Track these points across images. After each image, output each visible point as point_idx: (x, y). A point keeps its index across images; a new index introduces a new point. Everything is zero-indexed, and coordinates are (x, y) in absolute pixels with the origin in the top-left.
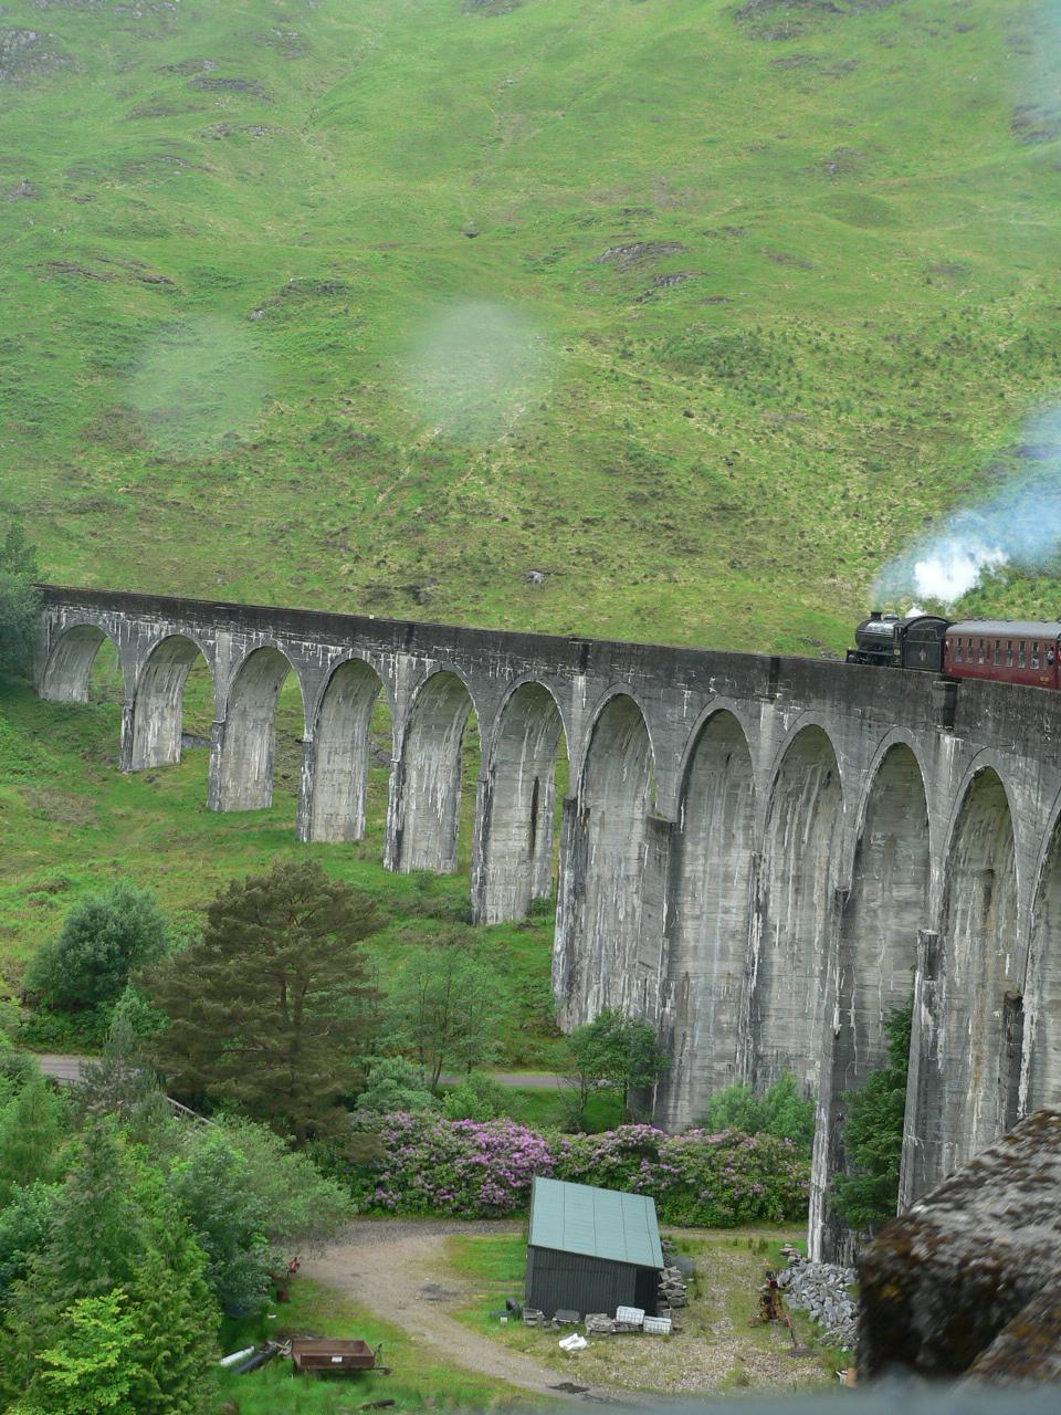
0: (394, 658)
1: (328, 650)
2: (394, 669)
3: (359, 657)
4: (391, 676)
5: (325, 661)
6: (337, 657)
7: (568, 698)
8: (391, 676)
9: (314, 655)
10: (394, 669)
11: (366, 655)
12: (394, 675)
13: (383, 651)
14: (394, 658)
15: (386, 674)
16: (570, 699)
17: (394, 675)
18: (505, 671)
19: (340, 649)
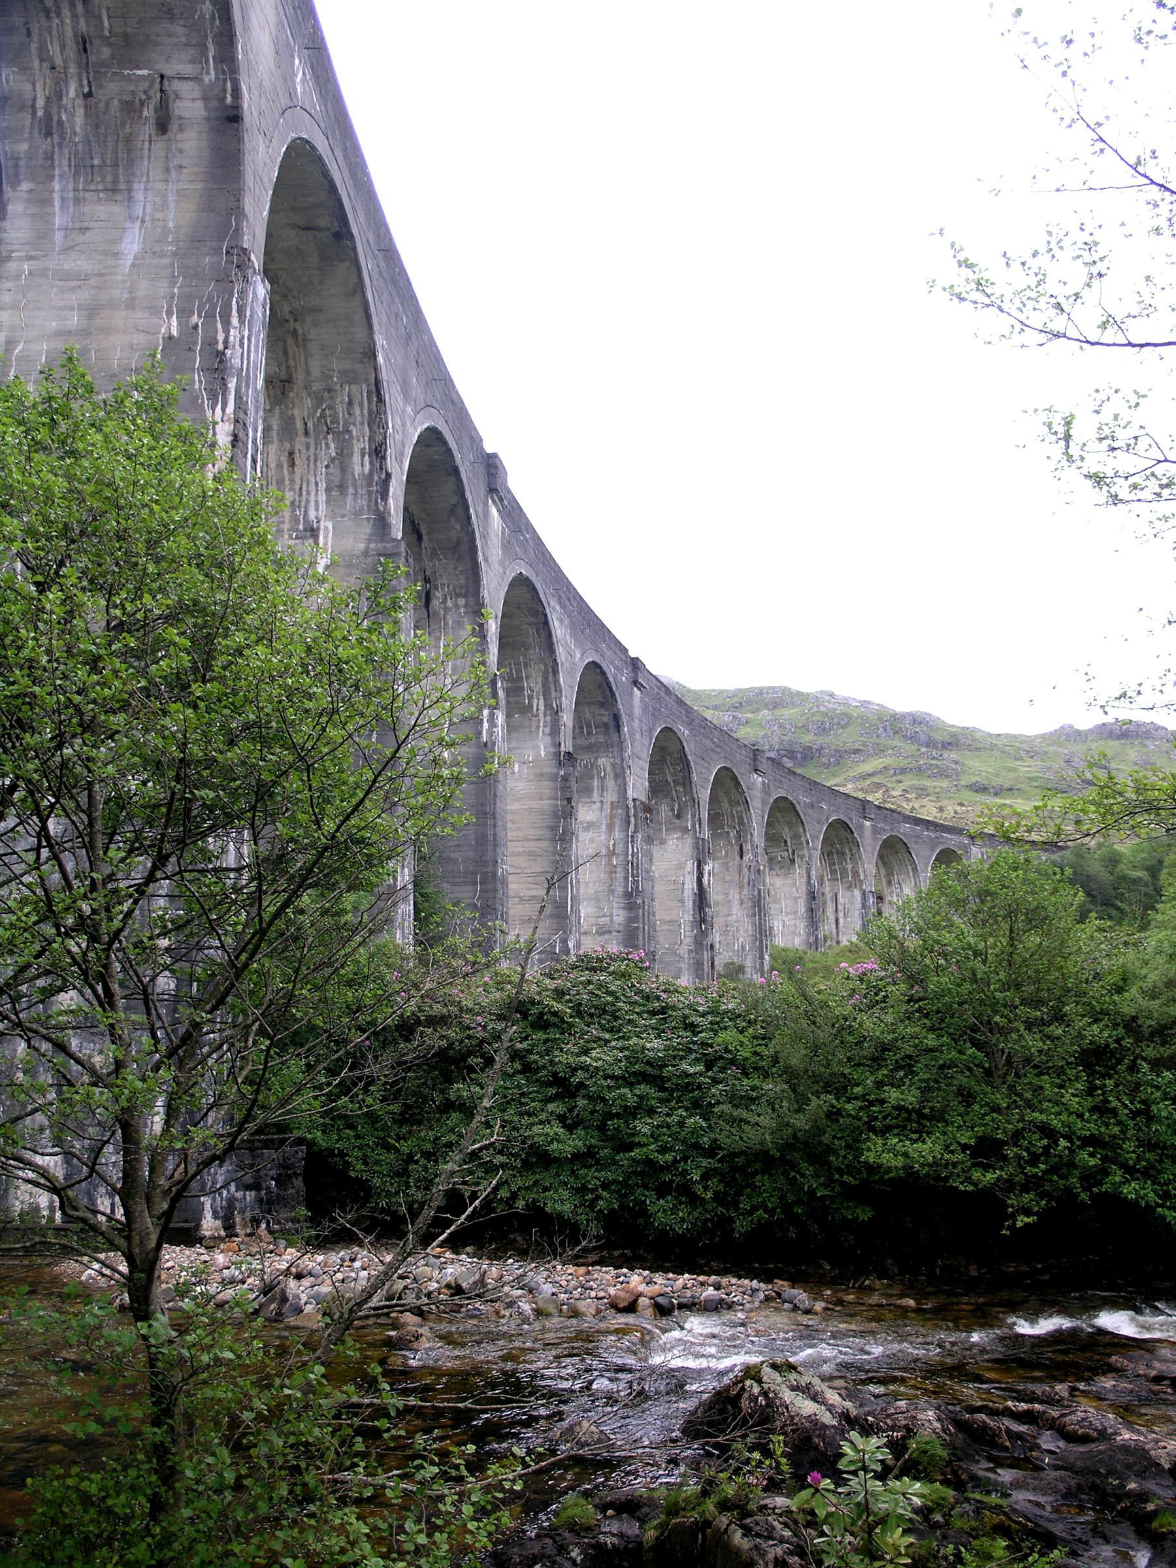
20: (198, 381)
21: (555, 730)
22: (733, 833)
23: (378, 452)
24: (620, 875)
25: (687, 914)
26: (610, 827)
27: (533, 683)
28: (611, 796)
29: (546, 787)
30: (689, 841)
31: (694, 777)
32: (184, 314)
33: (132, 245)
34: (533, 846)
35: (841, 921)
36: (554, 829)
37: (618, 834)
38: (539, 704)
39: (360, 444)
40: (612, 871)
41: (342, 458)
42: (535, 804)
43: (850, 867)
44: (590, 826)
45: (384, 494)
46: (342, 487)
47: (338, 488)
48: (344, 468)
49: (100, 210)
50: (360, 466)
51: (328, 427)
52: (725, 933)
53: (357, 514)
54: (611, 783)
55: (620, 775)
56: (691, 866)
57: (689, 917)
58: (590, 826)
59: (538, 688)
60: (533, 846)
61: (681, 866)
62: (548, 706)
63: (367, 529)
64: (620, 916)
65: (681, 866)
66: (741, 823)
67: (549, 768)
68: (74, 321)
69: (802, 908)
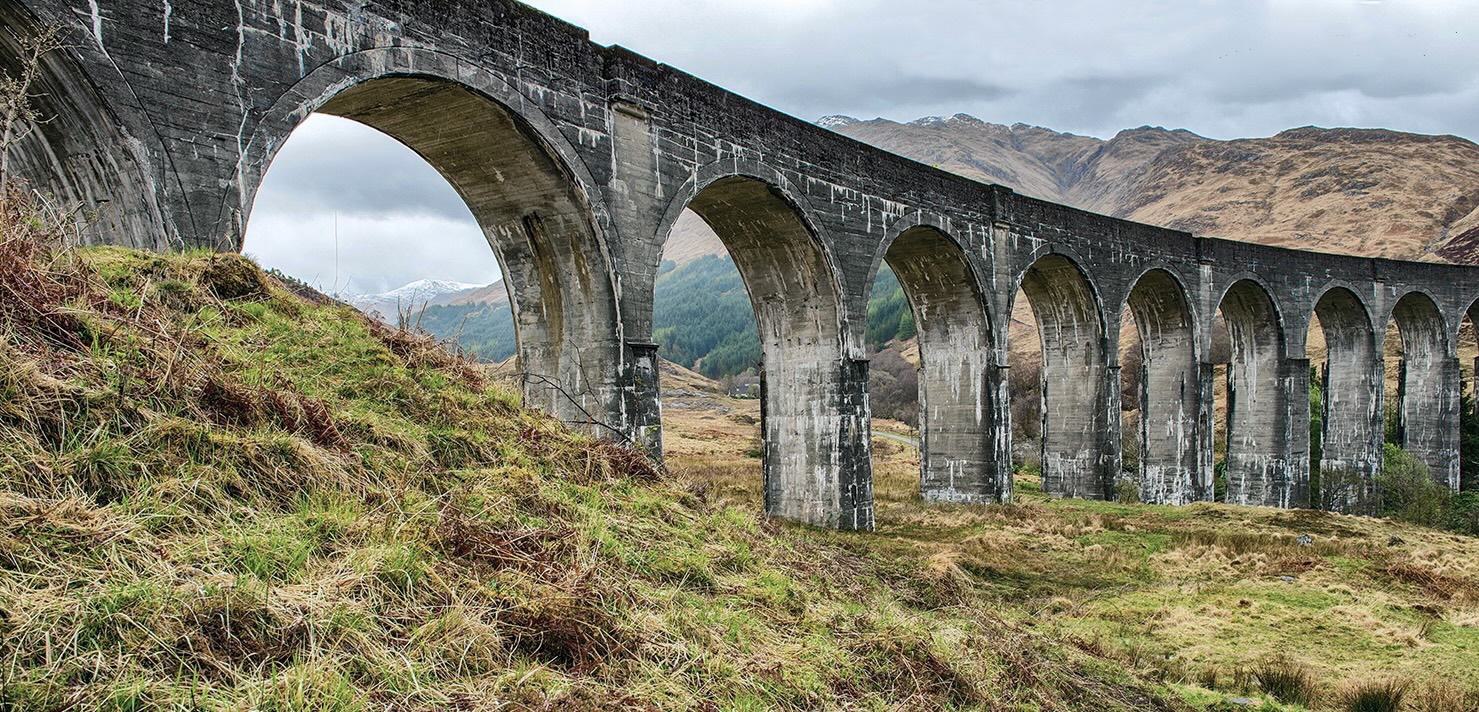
0: (987, 231)
1: (881, 207)
2: (988, 246)
3: (933, 224)
4: (985, 256)
5: (877, 223)
6: (896, 219)
7: (1197, 280)
8: (985, 256)
9: (856, 210)
10: (988, 246)
11: (944, 223)
12: (989, 256)
13: (970, 220)
14: (987, 231)
15: (977, 252)
16: (1198, 284)
17: (989, 256)
18: (1129, 257)
19: (901, 207)
20: (1368, 388)
23: (1443, 334)
32: (1365, 374)
33: (1354, 359)
41: (1433, 336)
45: (1447, 345)
46: (1434, 343)
47: (1433, 343)
49: (1347, 352)
50: (1439, 338)
51: (1426, 329)
53: (1439, 351)
63: (1442, 355)
68: (1344, 376)
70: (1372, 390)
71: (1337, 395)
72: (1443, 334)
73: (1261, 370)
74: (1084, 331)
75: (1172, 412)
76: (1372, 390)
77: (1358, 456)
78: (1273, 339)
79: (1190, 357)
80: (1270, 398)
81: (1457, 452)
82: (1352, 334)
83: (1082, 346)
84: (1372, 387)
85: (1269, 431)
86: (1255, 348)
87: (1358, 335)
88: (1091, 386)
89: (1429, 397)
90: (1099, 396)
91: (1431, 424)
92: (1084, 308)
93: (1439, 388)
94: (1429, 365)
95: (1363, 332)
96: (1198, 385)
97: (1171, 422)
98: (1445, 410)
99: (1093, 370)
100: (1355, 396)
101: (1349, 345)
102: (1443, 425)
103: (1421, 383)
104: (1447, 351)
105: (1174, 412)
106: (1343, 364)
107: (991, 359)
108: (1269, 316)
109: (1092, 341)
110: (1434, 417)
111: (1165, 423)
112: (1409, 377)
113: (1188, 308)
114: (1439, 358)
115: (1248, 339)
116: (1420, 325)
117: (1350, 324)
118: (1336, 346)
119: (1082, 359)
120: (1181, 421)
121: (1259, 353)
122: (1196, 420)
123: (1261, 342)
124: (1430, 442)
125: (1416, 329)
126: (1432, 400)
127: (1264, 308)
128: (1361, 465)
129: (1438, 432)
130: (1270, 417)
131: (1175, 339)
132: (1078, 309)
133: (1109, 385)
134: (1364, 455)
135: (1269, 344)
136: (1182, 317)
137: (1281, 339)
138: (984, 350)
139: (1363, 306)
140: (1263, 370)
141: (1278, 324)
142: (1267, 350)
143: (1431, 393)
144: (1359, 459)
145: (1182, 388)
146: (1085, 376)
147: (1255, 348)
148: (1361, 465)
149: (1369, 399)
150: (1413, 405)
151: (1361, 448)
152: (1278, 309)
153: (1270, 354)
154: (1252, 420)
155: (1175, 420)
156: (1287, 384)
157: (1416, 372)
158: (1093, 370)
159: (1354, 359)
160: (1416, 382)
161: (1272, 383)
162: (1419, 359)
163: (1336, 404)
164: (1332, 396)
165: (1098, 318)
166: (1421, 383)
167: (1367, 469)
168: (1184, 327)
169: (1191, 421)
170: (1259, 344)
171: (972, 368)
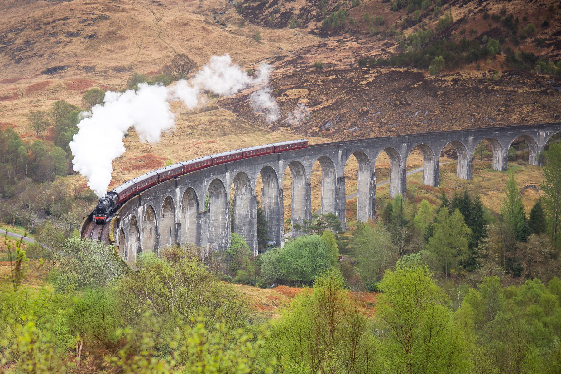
21: (306, 180)
22: (397, 160)
23: (250, 186)
24: (334, 194)
25: (367, 191)
26: (332, 184)
27: (301, 171)
28: (333, 177)
29: (304, 190)
30: (369, 173)
31: (369, 158)
33: (219, 203)
34: (302, 200)
35: (461, 169)
36: (305, 198)
37: (334, 185)
38: (302, 174)
39: (248, 185)
40: (333, 193)
42: (302, 193)
43: (464, 152)
44: (328, 183)
47: (247, 189)
48: (247, 187)
49: (217, 200)
50: (249, 187)
51: (244, 184)
52: (394, 187)
54: (332, 174)
55: (334, 172)
56: (369, 179)
57: (368, 192)
58: (328, 183)
59: (302, 172)
60: (302, 200)
61: (367, 179)
62: (304, 175)
63: (250, 195)
64: (334, 203)
65: (367, 179)
66: (398, 158)
67: (305, 186)
69: (432, 172)
70: (226, 216)
71: (213, 217)
72: (250, 186)
73: (191, 216)
74: (150, 223)
75: (167, 240)
76: (226, 216)
77: (222, 242)
78: (195, 205)
79: (173, 221)
80: (194, 227)
81: (256, 234)
82: (218, 193)
83: (149, 228)
84: (226, 214)
85: (194, 240)
86: (188, 208)
87: (221, 193)
88: (152, 241)
89: (245, 211)
90: (155, 245)
91: (246, 223)
92: (151, 217)
93: (249, 209)
94: (245, 198)
95: (223, 193)
96: (176, 231)
97: (167, 244)
98: (251, 218)
99: (153, 236)
100: (220, 217)
101: (217, 197)
102: (251, 223)
103: (242, 205)
104: (251, 193)
105: (168, 240)
106: (215, 204)
107: (139, 246)
108: (194, 197)
109: (153, 227)
110: (248, 220)
111: (165, 244)
112: (238, 202)
113: (173, 205)
114: (249, 196)
115: (186, 204)
116: (241, 182)
117: (218, 189)
118: (213, 197)
119: (149, 232)
120: (170, 244)
121: (190, 209)
122: (176, 243)
123: (191, 206)
124: (246, 230)
125: (240, 183)
126: (247, 213)
127: (192, 194)
128: (223, 245)
129: (249, 227)
130: (195, 234)
131: (168, 214)
132: (149, 217)
133: (158, 241)
134: (224, 241)
135: (193, 206)
136: (171, 207)
137: (198, 205)
138: (137, 243)
139: (222, 184)
140: (191, 216)
141: (197, 200)
142: (193, 209)
143: (246, 210)
144: (222, 243)
145: (171, 232)
146: (150, 238)
147: (188, 208)
148: (223, 245)
149: (225, 219)
150: (240, 214)
151: (223, 239)
152: (197, 195)
153: (194, 210)
154: (188, 235)
155: (169, 243)
156: (200, 222)
157: (241, 201)
158: (153, 236)
159: (219, 203)
160: (241, 205)
161: (195, 221)
162: (241, 196)
163: (213, 220)
164: (212, 217)
165: (155, 220)
166: (242, 205)
167: (226, 247)
168: (171, 211)
169: (174, 244)
170: (190, 206)
171: (133, 248)
